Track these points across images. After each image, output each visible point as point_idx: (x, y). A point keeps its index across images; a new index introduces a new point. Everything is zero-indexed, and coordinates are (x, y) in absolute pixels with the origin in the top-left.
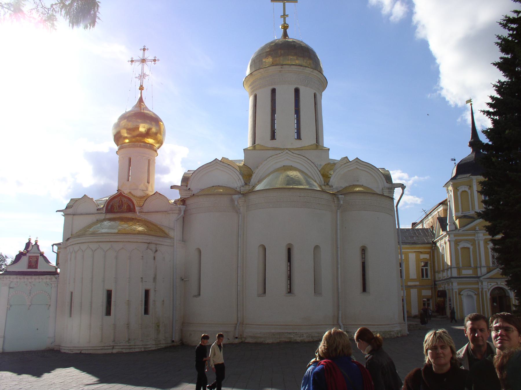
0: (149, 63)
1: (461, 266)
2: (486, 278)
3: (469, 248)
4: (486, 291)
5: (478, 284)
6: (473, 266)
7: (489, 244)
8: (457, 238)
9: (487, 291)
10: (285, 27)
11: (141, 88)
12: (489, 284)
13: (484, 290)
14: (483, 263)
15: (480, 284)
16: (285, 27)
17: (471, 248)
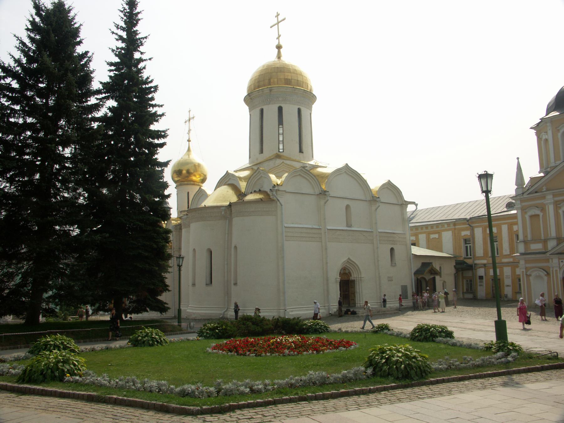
0: (191, 120)
1: (529, 237)
2: (556, 252)
3: (538, 215)
4: (557, 270)
5: (549, 262)
6: (543, 238)
7: (561, 208)
8: (524, 204)
9: (558, 269)
10: (279, 47)
11: (189, 141)
12: (561, 261)
13: (554, 270)
14: (553, 234)
15: (550, 261)
16: (279, 47)
17: (541, 214)
